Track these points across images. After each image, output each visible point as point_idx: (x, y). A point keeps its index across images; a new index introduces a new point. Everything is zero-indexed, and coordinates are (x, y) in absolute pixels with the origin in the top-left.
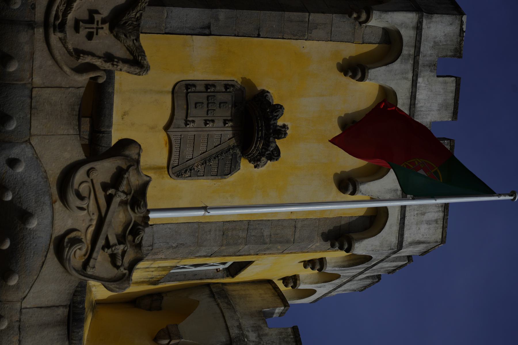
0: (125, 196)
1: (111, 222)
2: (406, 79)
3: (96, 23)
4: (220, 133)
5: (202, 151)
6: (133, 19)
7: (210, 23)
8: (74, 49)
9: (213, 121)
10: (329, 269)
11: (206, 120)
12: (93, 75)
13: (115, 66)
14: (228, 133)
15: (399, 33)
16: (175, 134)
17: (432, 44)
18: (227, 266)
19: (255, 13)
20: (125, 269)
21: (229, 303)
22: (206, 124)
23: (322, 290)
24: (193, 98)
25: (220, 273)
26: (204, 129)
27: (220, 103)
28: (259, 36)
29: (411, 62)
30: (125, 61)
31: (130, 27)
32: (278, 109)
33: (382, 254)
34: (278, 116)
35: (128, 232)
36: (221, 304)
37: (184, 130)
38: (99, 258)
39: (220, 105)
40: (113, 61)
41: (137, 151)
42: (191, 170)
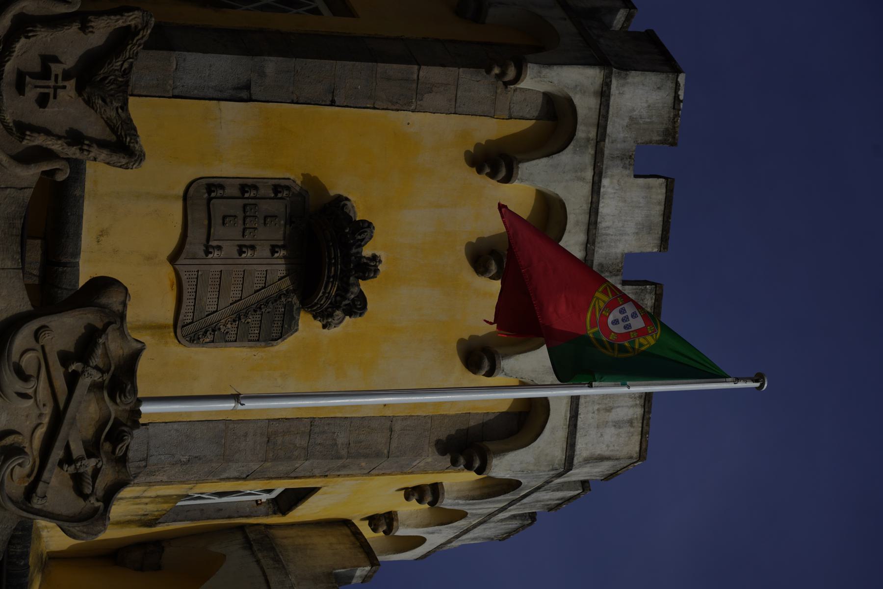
0: (100, 375)
1: (74, 418)
2: (583, 179)
3: (53, 78)
4: (264, 268)
5: (234, 299)
8: (14, 122)
9: (253, 248)
10: (448, 502)
11: (240, 247)
12: (46, 167)
13: (85, 153)
15: (570, 102)
17: (626, 121)
18: (273, 495)
19: (327, 64)
20: (98, 500)
21: (277, 560)
22: (241, 252)
23: (436, 537)
24: (220, 207)
26: (238, 261)
27: (265, 218)
28: (333, 104)
29: (591, 151)
30: (102, 144)
31: (112, 87)
32: (364, 228)
34: (363, 240)
35: (103, 437)
36: (262, 561)
37: (203, 261)
38: (54, 481)
39: (265, 221)
40: (83, 144)
41: (121, 298)
42: (214, 331)
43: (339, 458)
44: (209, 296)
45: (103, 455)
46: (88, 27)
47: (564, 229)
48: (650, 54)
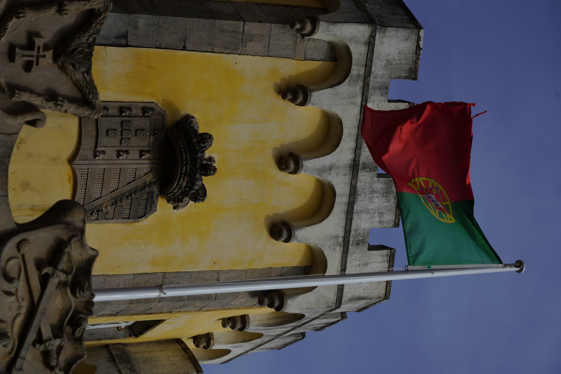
0: (65, 276)
1: (45, 309)
2: (354, 104)
4: (134, 166)
5: (113, 189)
6: (84, 45)
7: (127, 32)
8: (6, 83)
9: (127, 152)
10: (251, 328)
11: (118, 151)
13: (59, 107)
16: (81, 166)
17: (384, 62)
19: (181, 20)
20: (60, 370)
22: (119, 156)
25: (121, 332)
27: (136, 131)
28: (184, 49)
29: (361, 84)
30: (72, 100)
32: (206, 139)
33: (316, 312)
34: (205, 147)
35: (66, 322)
36: (123, 371)
38: (29, 357)
39: (136, 133)
42: (98, 211)
44: (95, 187)
45: (65, 336)
46: (64, 10)
47: (341, 139)
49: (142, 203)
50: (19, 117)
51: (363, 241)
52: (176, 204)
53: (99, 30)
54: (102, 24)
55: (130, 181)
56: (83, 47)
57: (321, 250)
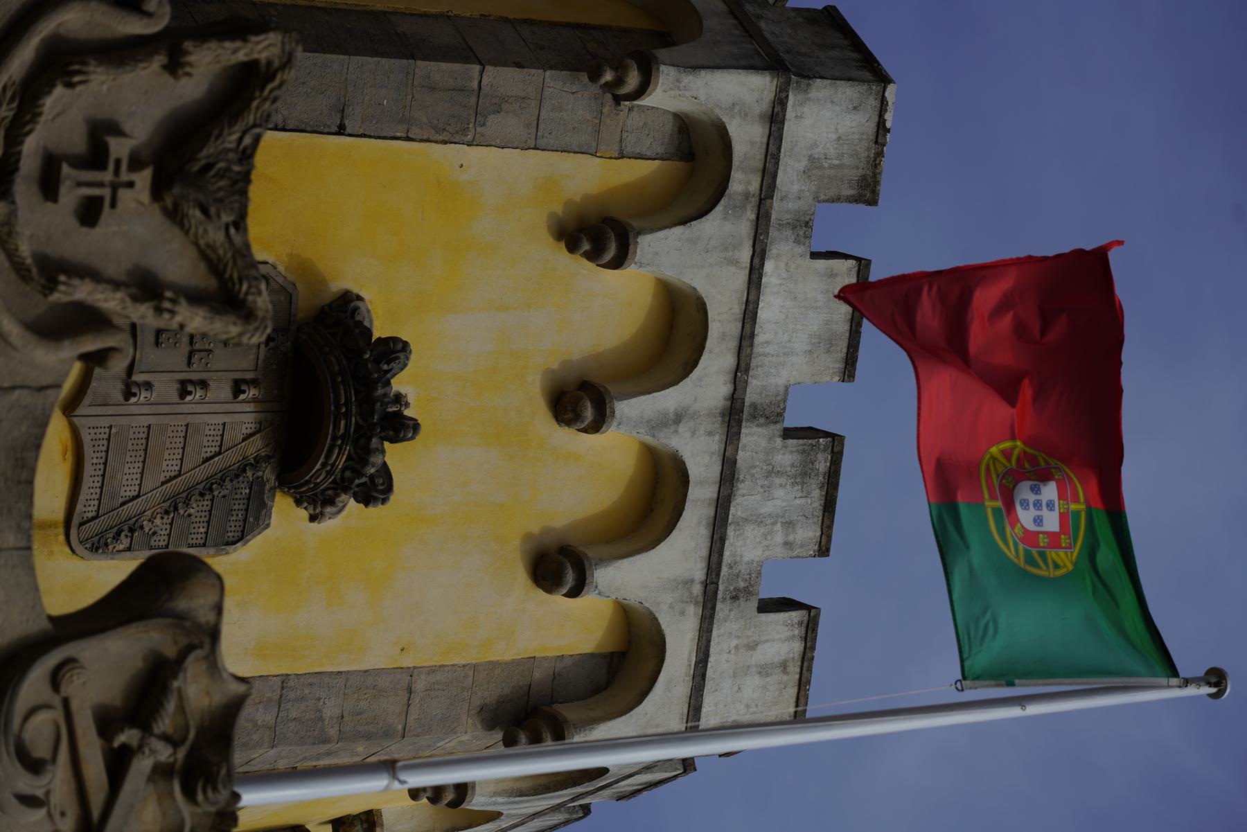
0: (170, 750)
2: (734, 262)
3: (111, 166)
4: (221, 419)
5: (168, 475)
6: (231, 156)
9: (203, 384)
10: (477, 803)
11: (183, 383)
12: (91, 345)
13: (166, 316)
14: (243, 418)
15: (722, 133)
17: (805, 162)
19: (335, 61)
22: (184, 393)
28: (341, 131)
34: (390, 370)
37: (119, 410)
41: (212, 598)
42: (132, 530)
43: (326, 741)
44: (127, 471)
47: (703, 348)
48: (835, 49)
49: (236, 507)
50: (67, 343)
51: (748, 592)
52: (317, 511)
53: (269, 115)
54: (275, 100)
55: (209, 455)
56: (228, 161)
57: (652, 614)
